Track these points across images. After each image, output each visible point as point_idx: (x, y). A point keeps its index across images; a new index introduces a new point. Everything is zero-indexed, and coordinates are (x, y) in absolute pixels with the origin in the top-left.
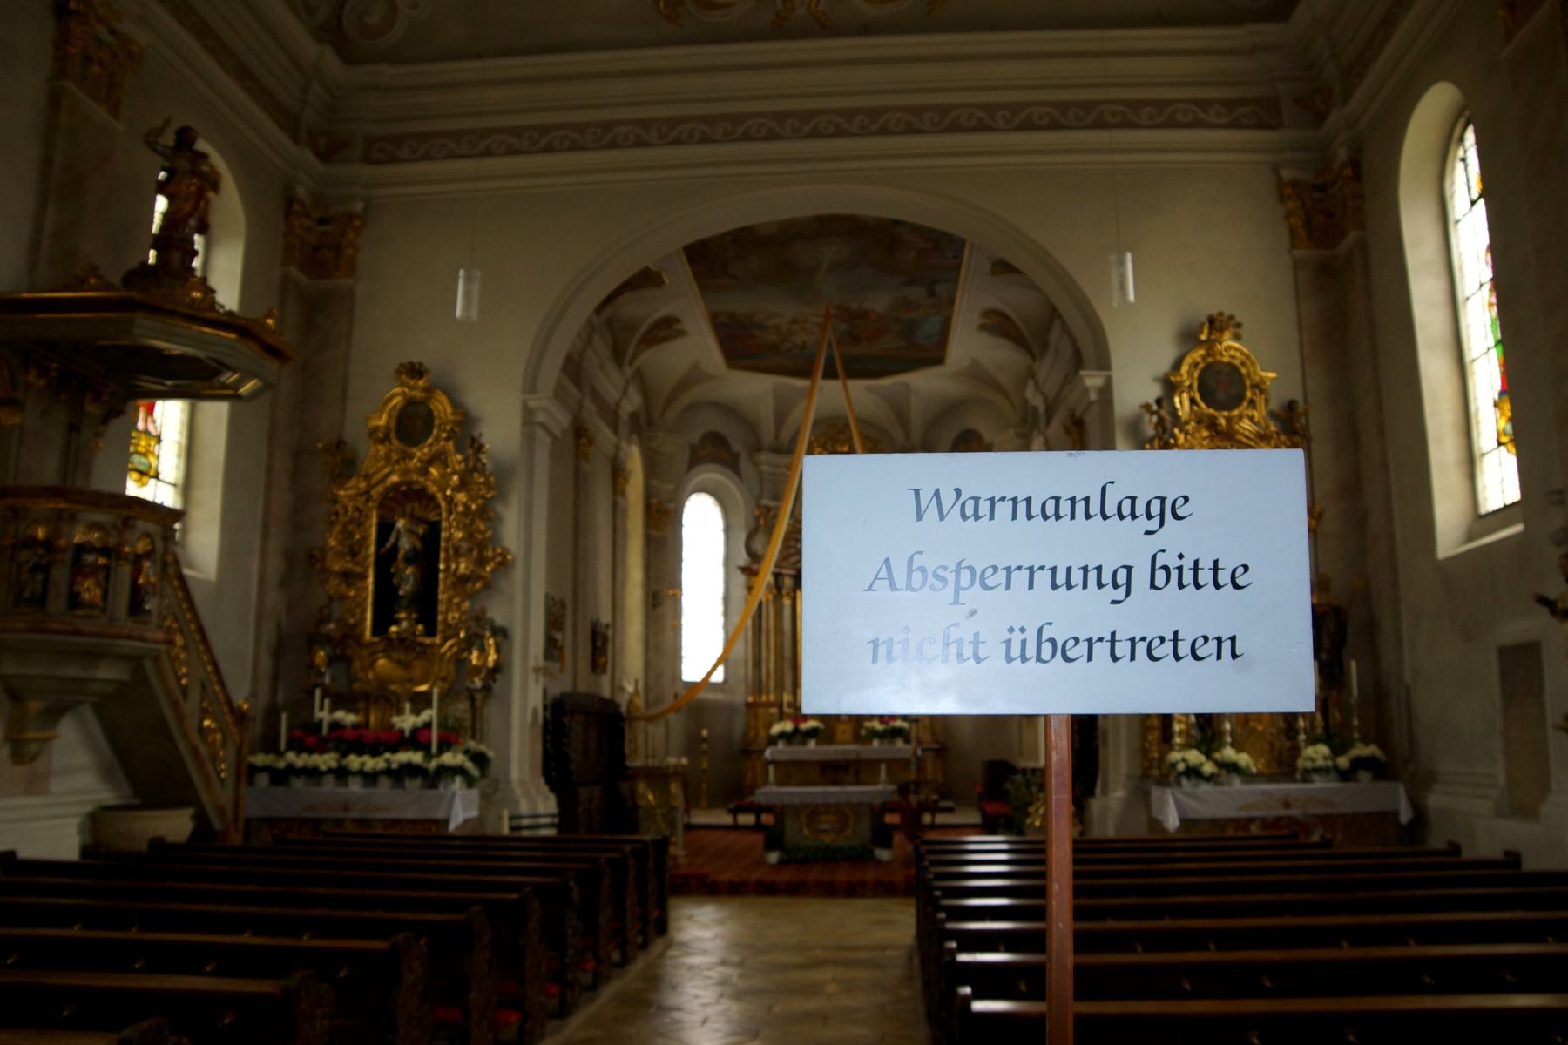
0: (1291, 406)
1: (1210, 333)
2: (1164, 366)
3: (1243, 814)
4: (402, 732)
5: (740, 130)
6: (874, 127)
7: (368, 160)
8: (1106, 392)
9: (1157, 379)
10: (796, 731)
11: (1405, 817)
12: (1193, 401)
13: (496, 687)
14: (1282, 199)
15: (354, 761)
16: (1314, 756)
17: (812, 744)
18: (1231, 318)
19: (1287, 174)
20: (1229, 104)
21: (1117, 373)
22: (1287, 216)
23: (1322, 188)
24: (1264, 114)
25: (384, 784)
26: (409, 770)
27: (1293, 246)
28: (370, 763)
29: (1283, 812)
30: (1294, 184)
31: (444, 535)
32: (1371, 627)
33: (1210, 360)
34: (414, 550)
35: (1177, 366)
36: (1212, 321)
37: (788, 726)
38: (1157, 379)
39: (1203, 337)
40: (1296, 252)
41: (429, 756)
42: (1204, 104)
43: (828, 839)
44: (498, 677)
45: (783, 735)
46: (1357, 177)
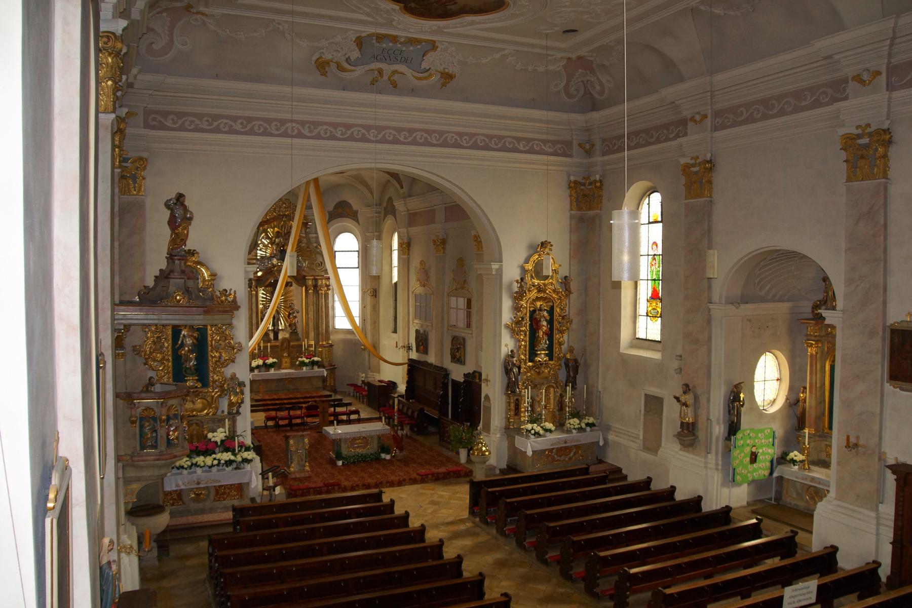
0: (566, 277)
1: (541, 249)
2: (522, 261)
3: (552, 447)
4: (216, 442)
5: (349, 133)
6: (410, 139)
7: (147, 126)
8: (500, 271)
9: (518, 266)
10: (265, 364)
11: (601, 444)
12: (532, 276)
13: (241, 410)
14: (570, 187)
15: (200, 460)
16: (575, 424)
17: (272, 371)
18: (550, 242)
19: (572, 178)
20: (554, 143)
21: (505, 264)
22: (571, 196)
23: (584, 184)
24: (563, 148)
25: (215, 469)
26: (229, 463)
27: (571, 209)
28: (209, 460)
29: (564, 445)
30: (575, 182)
31: (209, 339)
32: (587, 366)
33: (539, 259)
34: (193, 345)
35: (527, 261)
36: (542, 244)
37: (261, 362)
38: (518, 266)
39: (539, 250)
40: (572, 212)
41: (235, 454)
42: (544, 142)
43: (360, 451)
44: (242, 405)
45: (258, 367)
46: (600, 188)
